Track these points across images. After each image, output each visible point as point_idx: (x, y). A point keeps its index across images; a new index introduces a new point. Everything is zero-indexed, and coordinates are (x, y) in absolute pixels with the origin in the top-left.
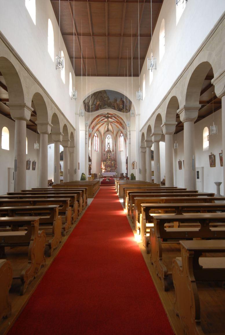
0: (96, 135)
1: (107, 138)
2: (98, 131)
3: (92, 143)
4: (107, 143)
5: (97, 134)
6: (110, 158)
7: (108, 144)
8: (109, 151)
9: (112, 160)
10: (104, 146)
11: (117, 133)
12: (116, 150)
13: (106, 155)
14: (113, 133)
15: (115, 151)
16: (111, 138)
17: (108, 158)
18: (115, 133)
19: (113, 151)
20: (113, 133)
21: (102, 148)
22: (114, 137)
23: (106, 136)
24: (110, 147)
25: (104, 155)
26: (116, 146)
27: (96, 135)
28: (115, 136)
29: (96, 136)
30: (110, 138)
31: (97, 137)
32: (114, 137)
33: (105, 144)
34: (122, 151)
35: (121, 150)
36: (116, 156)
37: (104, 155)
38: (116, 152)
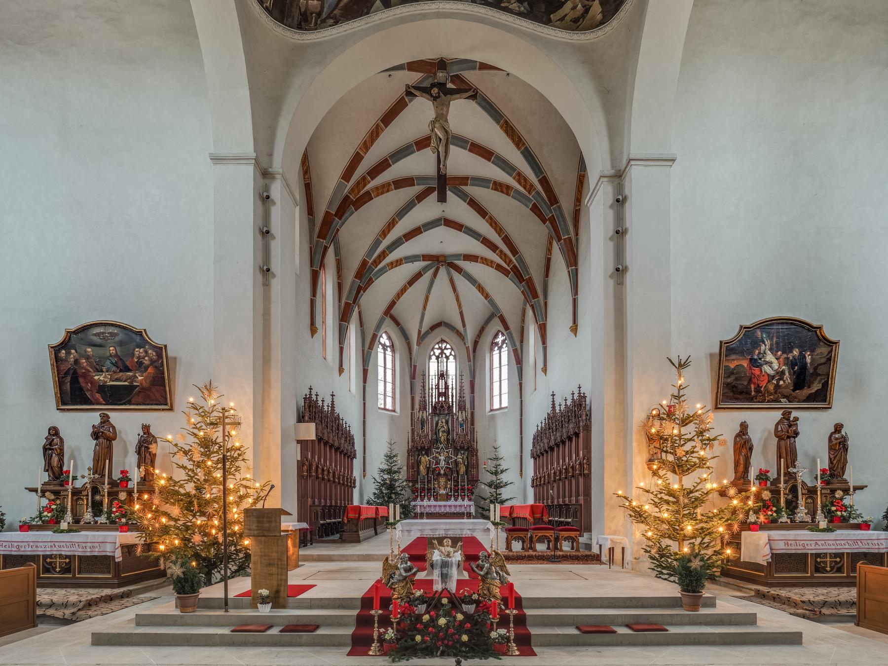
0: (388, 343)
1: (434, 358)
2: (397, 323)
3: (365, 372)
4: (433, 381)
5: (389, 338)
6: (448, 440)
7: (442, 376)
8: (442, 409)
9: (455, 448)
10: (424, 387)
11: (482, 331)
12: (473, 406)
13: (428, 429)
14: (461, 336)
15: (468, 406)
16: (451, 358)
17: (437, 440)
18: (470, 335)
19: (461, 407)
20: (461, 336)
21: (413, 399)
22: (467, 348)
23: (433, 349)
24: (447, 388)
25: (423, 423)
26: (472, 391)
27: (384, 340)
28: (470, 344)
29: (384, 346)
30: (447, 358)
31: (393, 351)
32: (467, 348)
33: (424, 375)
34: (501, 408)
35: (496, 406)
36: (473, 431)
37: (423, 423)
38: (472, 414)
